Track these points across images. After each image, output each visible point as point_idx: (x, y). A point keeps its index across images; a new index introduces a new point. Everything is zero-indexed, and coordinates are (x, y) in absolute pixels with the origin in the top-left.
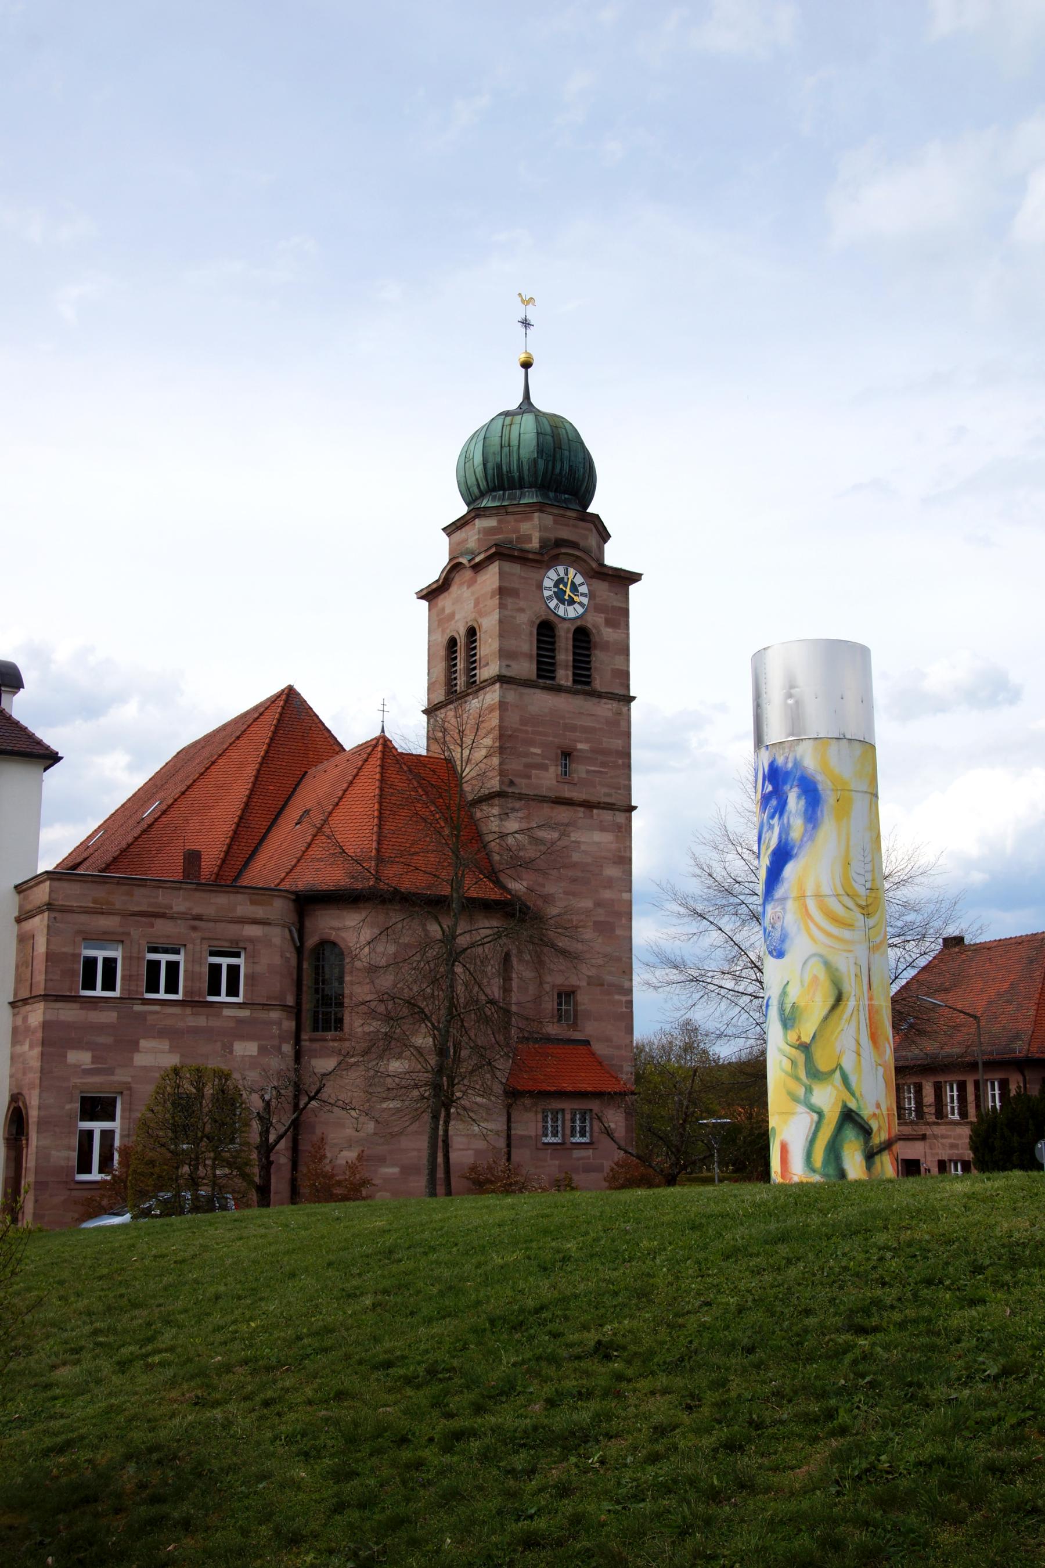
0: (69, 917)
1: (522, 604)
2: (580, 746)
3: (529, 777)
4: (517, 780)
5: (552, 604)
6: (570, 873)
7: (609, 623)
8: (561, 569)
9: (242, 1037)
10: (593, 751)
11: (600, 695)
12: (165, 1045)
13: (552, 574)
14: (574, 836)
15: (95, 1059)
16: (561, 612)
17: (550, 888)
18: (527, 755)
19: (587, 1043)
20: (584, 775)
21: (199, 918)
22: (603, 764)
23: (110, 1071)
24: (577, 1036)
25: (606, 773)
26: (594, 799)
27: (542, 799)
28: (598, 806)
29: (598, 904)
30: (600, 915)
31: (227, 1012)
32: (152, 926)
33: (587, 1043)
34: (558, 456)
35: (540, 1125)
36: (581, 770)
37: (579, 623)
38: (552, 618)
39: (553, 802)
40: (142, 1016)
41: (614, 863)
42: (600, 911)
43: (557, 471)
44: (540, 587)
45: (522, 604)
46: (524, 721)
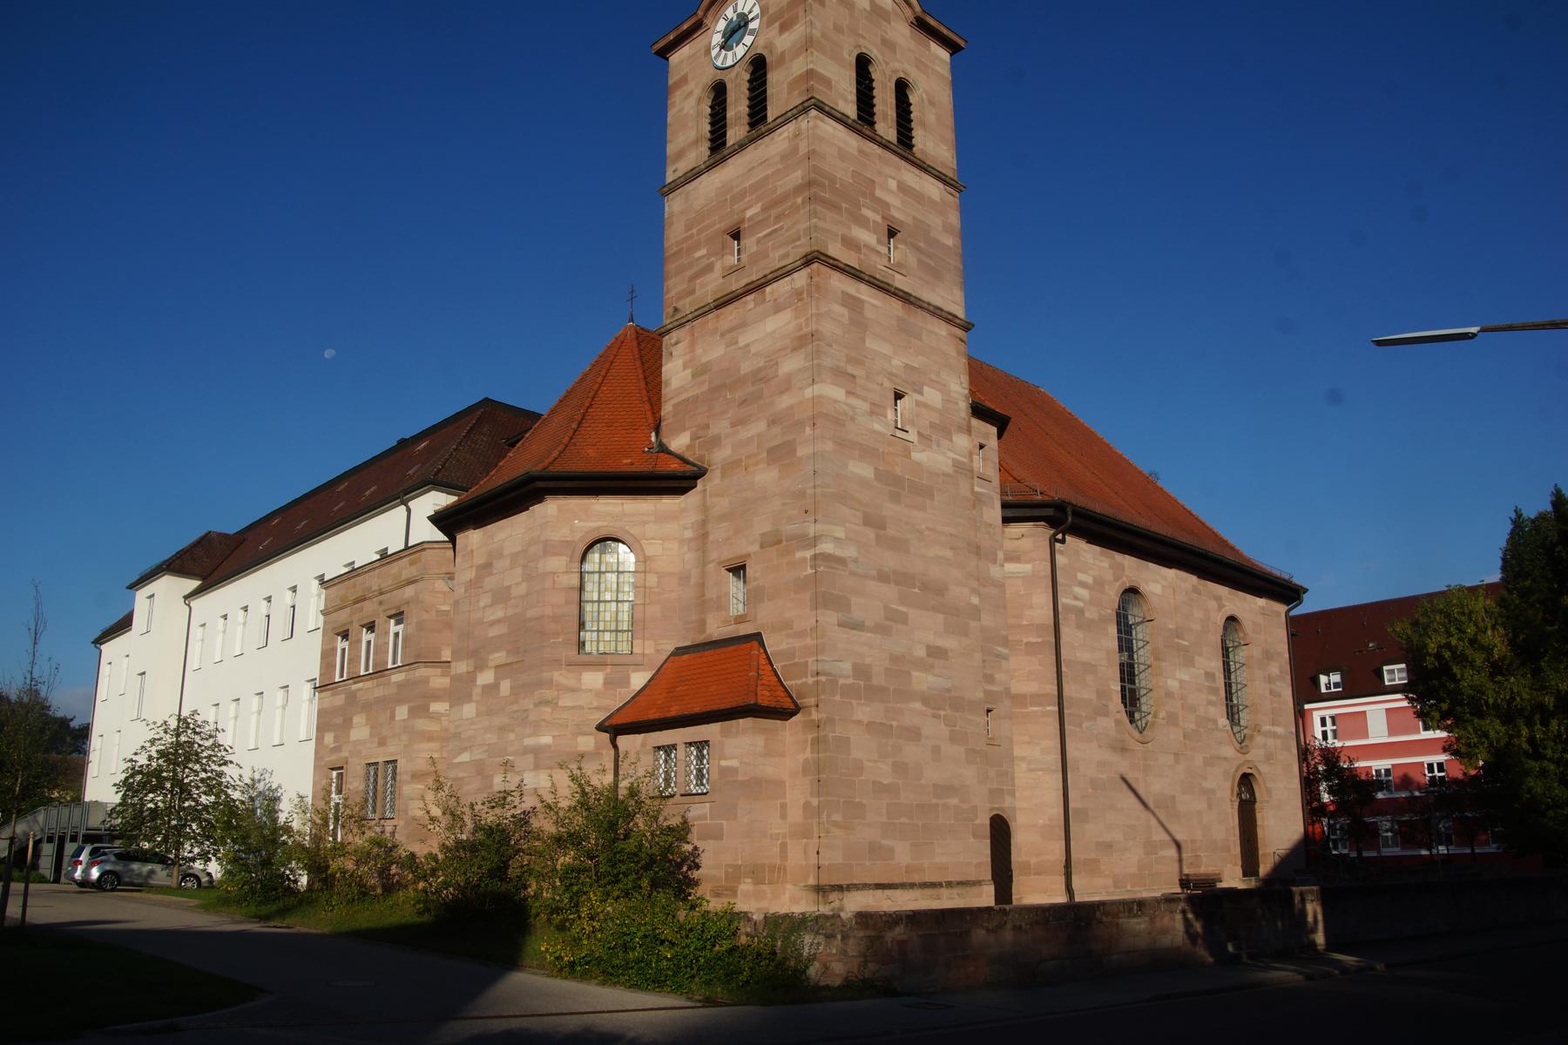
2: (749, 213)
4: (679, 305)
6: (739, 395)
7: (784, 28)
9: (400, 701)
10: (765, 209)
19: (757, 637)
20: (755, 249)
22: (778, 218)
27: (702, 312)
29: (772, 422)
33: (757, 637)
38: (720, 75)
39: (718, 307)
41: (794, 350)
42: (776, 430)
45: (691, 86)
46: (688, 228)
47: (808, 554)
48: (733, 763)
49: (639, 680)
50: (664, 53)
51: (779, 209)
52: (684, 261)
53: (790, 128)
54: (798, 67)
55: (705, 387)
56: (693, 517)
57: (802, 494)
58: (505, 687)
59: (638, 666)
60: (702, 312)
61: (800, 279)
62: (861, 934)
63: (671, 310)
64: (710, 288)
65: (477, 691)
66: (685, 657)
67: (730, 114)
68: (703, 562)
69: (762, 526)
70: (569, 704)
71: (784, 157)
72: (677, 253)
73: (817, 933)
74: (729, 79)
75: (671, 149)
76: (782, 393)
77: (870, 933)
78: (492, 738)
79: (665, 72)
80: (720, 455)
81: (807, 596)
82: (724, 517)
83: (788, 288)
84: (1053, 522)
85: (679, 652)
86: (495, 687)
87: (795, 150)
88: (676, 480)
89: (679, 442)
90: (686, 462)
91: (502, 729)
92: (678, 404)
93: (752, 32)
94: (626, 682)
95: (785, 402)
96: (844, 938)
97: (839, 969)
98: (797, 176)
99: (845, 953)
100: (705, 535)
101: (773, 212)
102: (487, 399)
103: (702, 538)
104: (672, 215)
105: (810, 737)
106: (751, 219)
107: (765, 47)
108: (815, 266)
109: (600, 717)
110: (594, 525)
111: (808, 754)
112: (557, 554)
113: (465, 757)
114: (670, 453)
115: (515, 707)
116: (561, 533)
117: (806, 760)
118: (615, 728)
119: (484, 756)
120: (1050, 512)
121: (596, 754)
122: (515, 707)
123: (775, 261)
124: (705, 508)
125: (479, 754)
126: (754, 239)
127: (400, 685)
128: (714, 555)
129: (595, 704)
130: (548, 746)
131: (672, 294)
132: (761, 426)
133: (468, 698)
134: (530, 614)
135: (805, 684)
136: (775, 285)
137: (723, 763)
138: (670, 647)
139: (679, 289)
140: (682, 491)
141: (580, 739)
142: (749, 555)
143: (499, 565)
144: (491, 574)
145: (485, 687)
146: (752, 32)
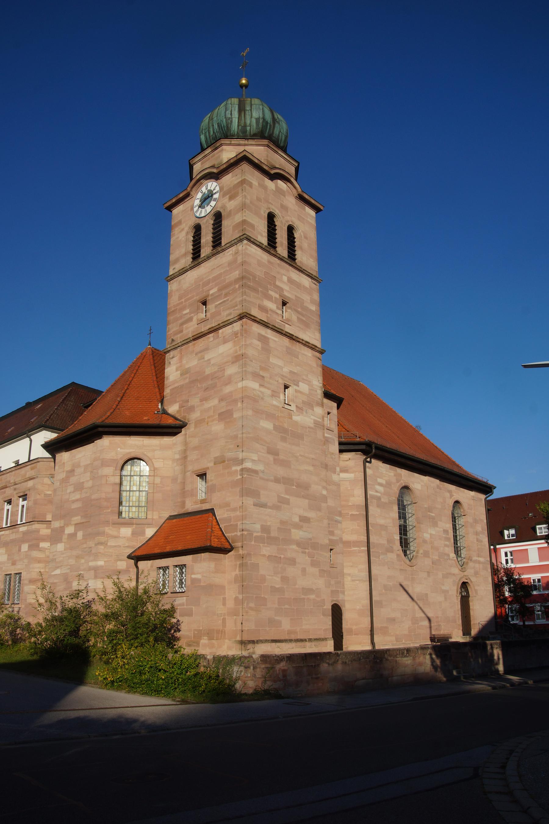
2: (211, 292)
4: (174, 338)
6: (204, 385)
7: (231, 198)
8: (204, 189)
9: (24, 541)
10: (219, 290)
14: (207, 358)
19: (212, 511)
20: (214, 310)
22: (226, 295)
25: (228, 300)
27: (187, 342)
29: (221, 400)
32: (5, 492)
33: (212, 511)
34: (211, 125)
37: (212, 212)
38: (198, 221)
39: (194, 340)
41: (233, 363)
42: (223, 404)
43: (212, 133)
45: (183, 226)
46: (180, 298)
47: (239, 468)
48: (198, 576)
49: (150, 532)
50: (170, 208)
51: (226, 291)
52: (178, 315)
53: (234, 249)
54: (238, 218)
55: (187, 381)
56: (180, 448)
57: (236, 437)
58: (80, 535)
59: (150, 525)
60: (187, 342)
61: (237, 326)
62: (263, 666)
63: (170, 340)
64: (191, 329)
65: (65, 537)
66: (174, 520)
67: (203, 241)
68: (184, 472)
69: (215, 453)
70: (114, 544)
71: (230, 264)
72: (173, 311)
73: (241, 666)
74: (203, 223)
75: (172, 257)
76: (227, 384)
77: (269, 666)
78: (72, 562)
79: (170, 218)
80: (194, 416)
81: (238, 489)
83: (230, 331)
84: (365, 452)
85: (171, 518)
87: (235, 261)
88: (172, 429)
89: (173, 409)
90: (176, 419)
91: (78, 557)
92: (173, 389)
93: (215, 200)
94: (143, 533)
95: (228, 389)
96: (254, 669)
97: (251, 684)
98: (236, 274)
99: (254, 675)
100: (185, 458)
101: (224, 292)
102: (73, 383)
104: (172, 291)
105: (238, 563)
106: (212, 295)
107: (222, 208)
108: (245, 320)
109: (129, 551)
110: (128, 451)
111: (237, 572)
112: (108, 466)
113: (58, 572)
114: (168, 414)
115: (85, 546)
116: (110, 455)
117: (236, 575)
118: (137, 558)
119: (68, 571)
120: (363, 447)
121: (127, 571)
122: (85, 546)
123: (224, 316)
124: (186, 443)
125: (65, 570)
126: (213, 305)
127: (24, 533)
128: (190, 468)
129: (127, 545)
130: (102, 566)
131: (171, 332)
133: (60, 540)
134: (93, 497)
135: (236, 535)
136: (224, 329)
137: (193, 576)
138: (166, 515)
139: (175, 329)
140: (174, 434)
141: (119, 563)
142: (208, 468)
143: (78, 471)
144: (74, 475)
146: (215, 200)
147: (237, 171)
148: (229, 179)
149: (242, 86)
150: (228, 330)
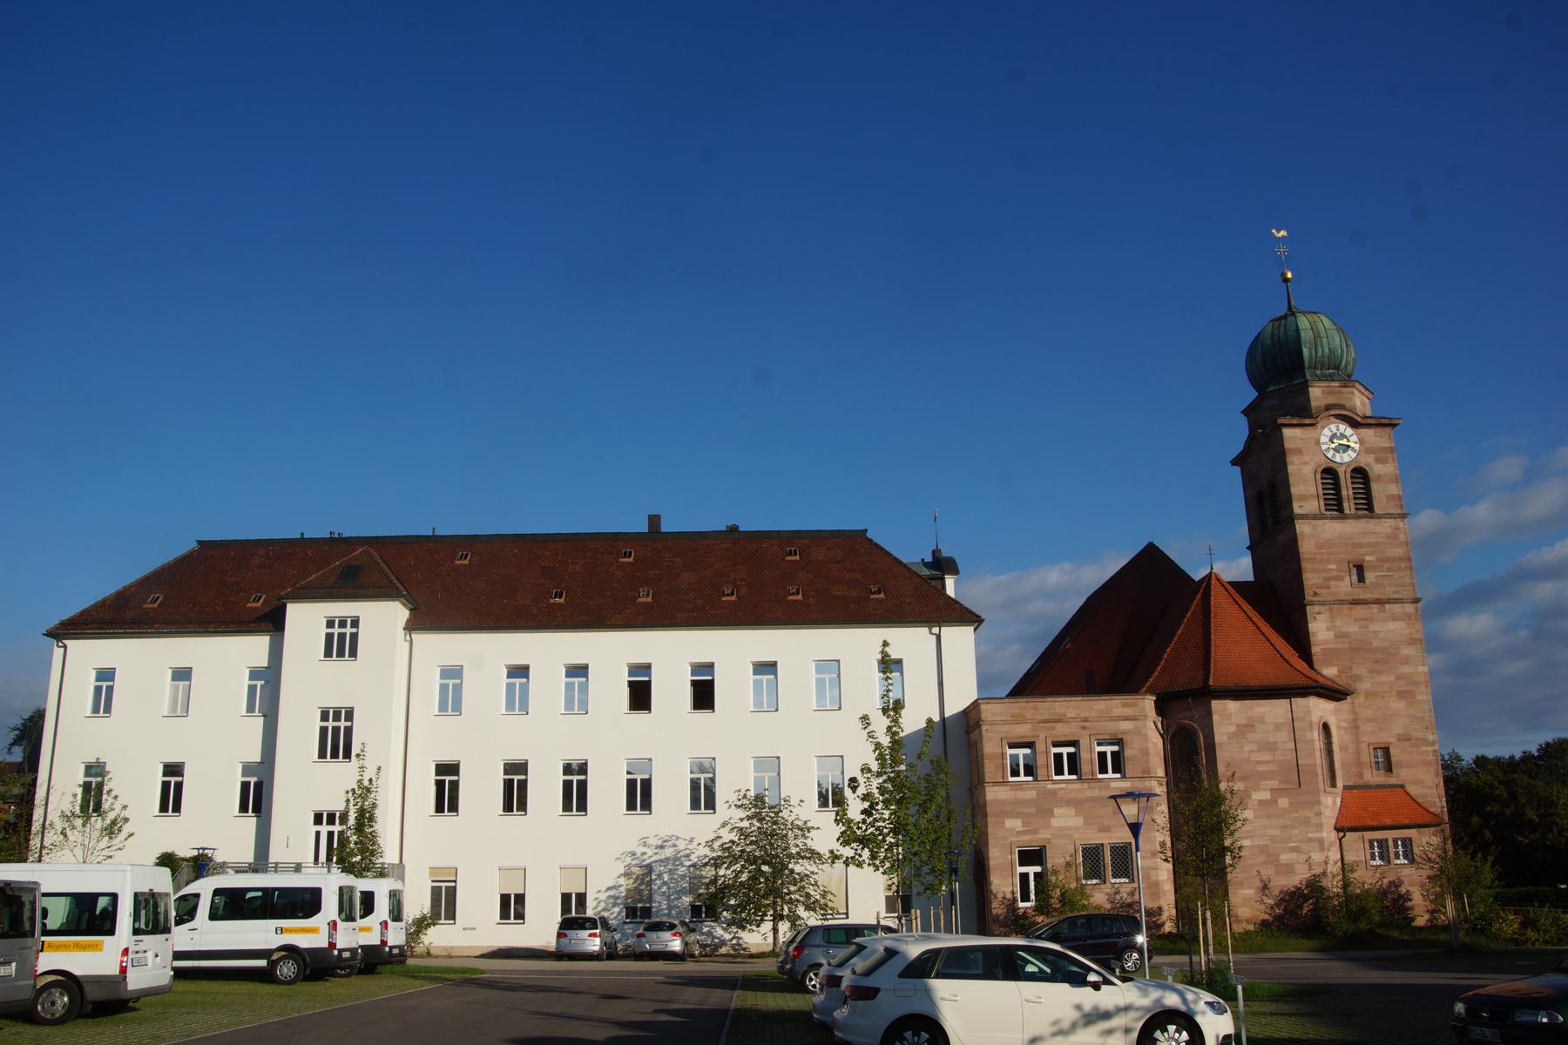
0: (996, 728)
1: (1306, 459)
3: (1328, 587)
5: (1330, 455)
7: (1378, 460)
8: (1333, 427)
10: (1379, 560)
11: (1379, 517)
12: (1072, 811)
13: (1327, 432)
14: (1373, 627)
15: (1024, 824)
16: (1338, 459)
17: (1361, 670)
18: (1325, 571)
19: (1402, 786)
21: (1086, 720)
22: (1389, 569)
23: (1035, 832)
24: (1393, 780)
26: (1385, 597)
27: (1341, 602)
28: (1389, 601)
29: (1399, 677)
30: (1401, 685)
31: (1113, 785)
35: (1368, 852)
36: (1370, 576)
38: (1331, 465)
40: (1054, 793)
42: (1401, 682)
44: (1318, 443)
45: (1306, 459)
46: (1319, 546)
53: (1390, 522)
56: (1346, 716)
57: (1422, 719)
67: (1344, 493)
68: (1358, 742)
69: (1398, 727)
71: (1388, 537)
74: (1341, 470)
80: (1364, 686)
82: (1369, 720)
86: (1273, 802)
87: (1396, 537)
88: (1334, 693)
89: (1330, 671)
95: (1406, 669)
100: (1357, 728)
103: (1354, 727)
123: (1389, 591)
124: (1354, 712)
125: (1258, 842)
132: (1392, 678)
140: (1337, 700)
145: (1262, 802)
147: (1380, 430)
148: (1368, 433)
149: (1286, 280)
150: (1397, 608)
